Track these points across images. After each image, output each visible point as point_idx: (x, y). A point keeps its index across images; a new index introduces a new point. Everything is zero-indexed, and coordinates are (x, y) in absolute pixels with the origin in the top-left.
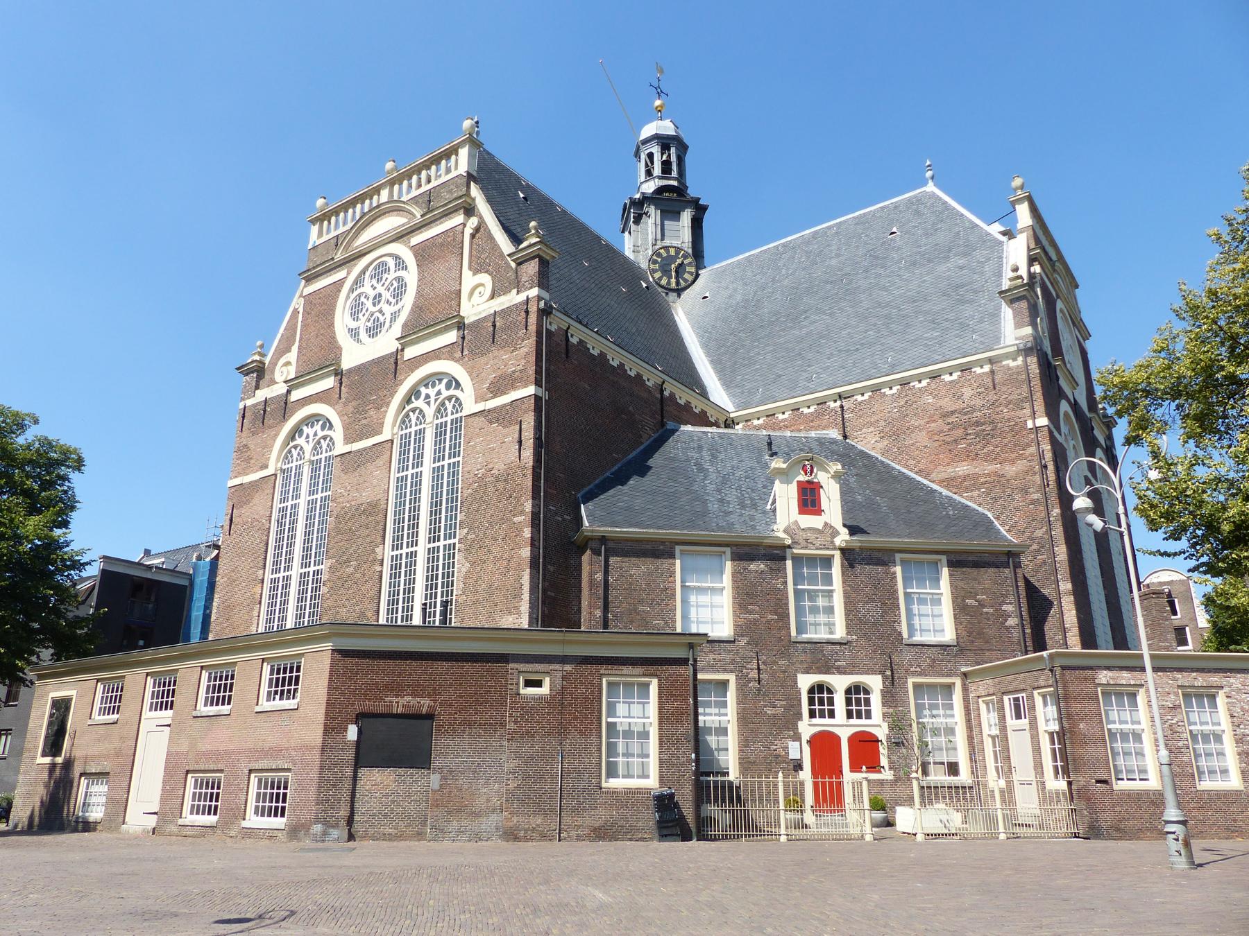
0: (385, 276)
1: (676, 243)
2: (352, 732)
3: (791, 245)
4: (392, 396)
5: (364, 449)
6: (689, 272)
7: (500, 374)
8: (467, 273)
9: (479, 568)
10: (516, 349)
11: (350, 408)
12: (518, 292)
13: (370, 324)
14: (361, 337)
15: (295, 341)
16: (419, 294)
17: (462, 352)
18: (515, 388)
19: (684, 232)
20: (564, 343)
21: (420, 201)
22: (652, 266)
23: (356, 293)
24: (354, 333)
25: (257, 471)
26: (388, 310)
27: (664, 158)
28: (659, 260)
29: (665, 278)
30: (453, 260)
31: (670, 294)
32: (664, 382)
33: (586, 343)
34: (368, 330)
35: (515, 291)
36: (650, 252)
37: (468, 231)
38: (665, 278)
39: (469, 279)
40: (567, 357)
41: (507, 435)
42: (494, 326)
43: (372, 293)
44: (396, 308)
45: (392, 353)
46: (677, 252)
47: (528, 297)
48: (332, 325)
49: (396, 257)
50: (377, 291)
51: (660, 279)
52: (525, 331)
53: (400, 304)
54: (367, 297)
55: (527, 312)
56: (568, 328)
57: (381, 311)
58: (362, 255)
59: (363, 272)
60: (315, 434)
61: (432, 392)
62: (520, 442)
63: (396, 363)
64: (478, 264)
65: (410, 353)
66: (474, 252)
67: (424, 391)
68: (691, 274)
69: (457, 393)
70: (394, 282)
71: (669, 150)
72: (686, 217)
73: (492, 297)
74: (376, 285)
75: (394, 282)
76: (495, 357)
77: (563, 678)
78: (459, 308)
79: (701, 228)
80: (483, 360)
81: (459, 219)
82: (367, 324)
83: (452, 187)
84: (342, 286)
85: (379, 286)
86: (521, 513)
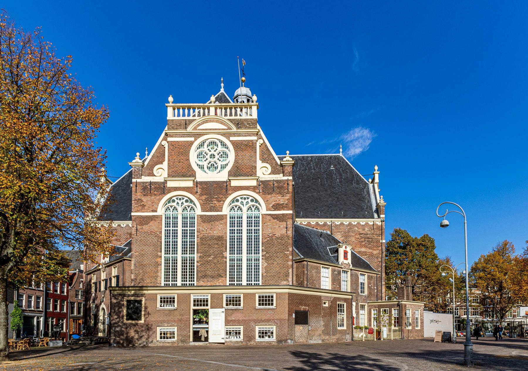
2: (294, 315)
4: (226, 198)
5: (213, 216)
9: (271, 266)
10: (283, 196)
11: (204, 197)
12: (284, 176)
16: (236, 162)
18: (284, 210)
23: (199, 150)
24: (201, 167)
25: (150, 212)
30: (252, 154)
35: (281, 175)
39: (259, 164)
41: (282, 225)
48: (188, 160)
60: (182, 203)
61: (245, 202)
62: (287, 228)
65: (234, 183)
67: (240, 200)
69: (257, 205)
77: (331, 302)
80: (269, 196)
81: (254, 138)
83: (249, 122)
86: (288, 251)
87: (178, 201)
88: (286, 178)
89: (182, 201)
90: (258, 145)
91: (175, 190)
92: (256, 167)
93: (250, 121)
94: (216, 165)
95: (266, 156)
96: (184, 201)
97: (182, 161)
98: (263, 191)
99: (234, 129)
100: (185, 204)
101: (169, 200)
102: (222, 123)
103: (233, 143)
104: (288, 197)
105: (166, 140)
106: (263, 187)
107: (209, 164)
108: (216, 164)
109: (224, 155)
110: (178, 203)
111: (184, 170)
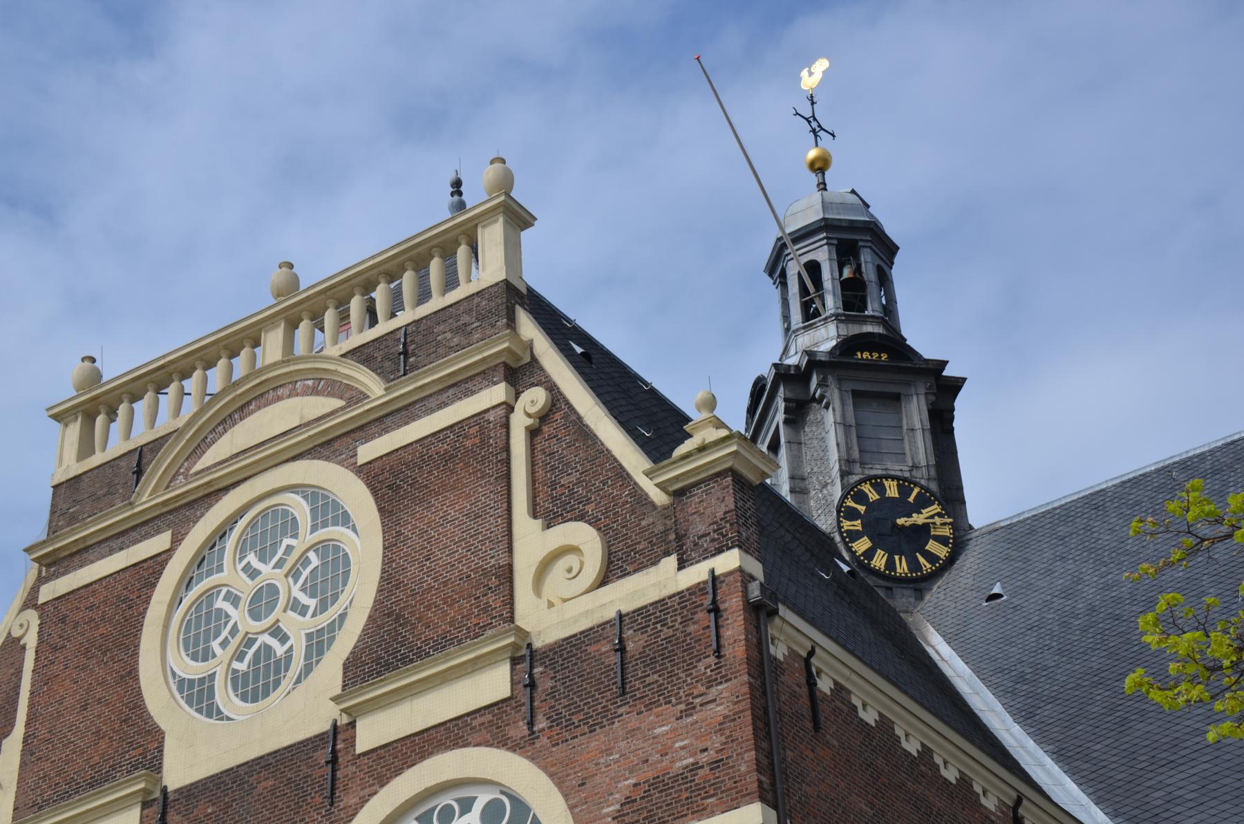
0: (287, 541)
1: (895, 468)
3: (1208, 465)
6: (937, 538)
7: (650, 775)
8: (525, 527)
10: (690, 709)
12: (682, 565)
13: (242, 666)
14: (219, 699)
15: (11, 724)
16: (390, 580)
17: (531, 724)
19: (913, 444)
20: (804, 691)
21: (379, 355)
22: (847, 525)
23: (197, 590)
26: (298, 628)
27: (847, 273)
28: (862, 509)
29: (880, 552)
31: (898, 592)
32: (1019, 802)
33: (849, 692)
34: (238, 682)
35: (671, 562)
36: (838, 492)
37: (519, 424)
38: (880, 552)
40: (817, 727)
42: (622, 649)
43: (246, 587)
44: (324, 620)
45: (321, 737)
46: (904, 490)
47: (712, 571)
48: (131, 674)
49: (312, 493)
50: (259, 582)
51: (869, 554)
52: (712, 660)
53: (333, 612)
54: (234, 600)
55: (715, 610)
56: (811, 653)
57: (276, 632)
58: (213, 494)
59: (221, 533)
63: (334, 761)
64: (554, 499)
66: (540, 473)
68: (943, 540)
70: (312, 555)
71: (856, 256)
72: (916, 412)
73: (604, 580)
74: (256, 564)
75: (312, 555)
76: (632, 733)
78: (512, 611)
79: (950, 432)
80: (598, 740)
82: (236, 665)
83: (465, 319)
84: (157, 574)
85: (265, 569)
88: (697, 573)
90: (519, 424)
92: (507, 574)
93: (469, 312)
95: (573, 479)
97: (99, 692)
98: (555, 720)
99: (374, 386)
102: (325, 385)
103: (372, 474)
104: (720, 710)
106: (552, 693)
107: (240, 657)
108: (284, 639)
111: (103, 744)
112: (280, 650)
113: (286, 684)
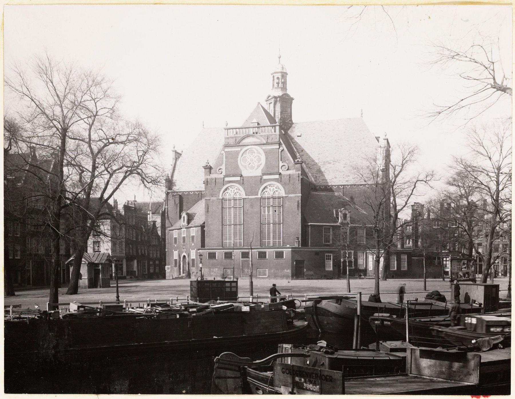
8: (280, 162)
24: (245, 167)
26: (256, 164)
59: (246, 150)
60: (234, 190)
61: (272, 188)
65: (265, 177)
85: (252, 156)
87: (232, 189)
89: (234, 189)
91: (229, 183)
94: (254, 165)
96: (235, 189)
100: (236, 191)
101: (226, 190)
103: (264, 150)
105: (224, 150)
109: (259, 160)
110: (231, 190)
112: (254, 165)
113: (255, 169)
